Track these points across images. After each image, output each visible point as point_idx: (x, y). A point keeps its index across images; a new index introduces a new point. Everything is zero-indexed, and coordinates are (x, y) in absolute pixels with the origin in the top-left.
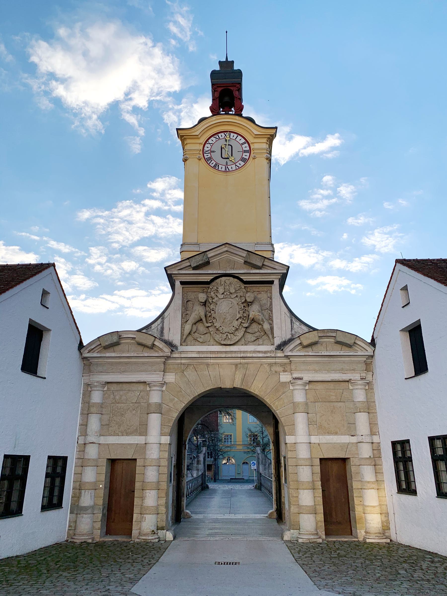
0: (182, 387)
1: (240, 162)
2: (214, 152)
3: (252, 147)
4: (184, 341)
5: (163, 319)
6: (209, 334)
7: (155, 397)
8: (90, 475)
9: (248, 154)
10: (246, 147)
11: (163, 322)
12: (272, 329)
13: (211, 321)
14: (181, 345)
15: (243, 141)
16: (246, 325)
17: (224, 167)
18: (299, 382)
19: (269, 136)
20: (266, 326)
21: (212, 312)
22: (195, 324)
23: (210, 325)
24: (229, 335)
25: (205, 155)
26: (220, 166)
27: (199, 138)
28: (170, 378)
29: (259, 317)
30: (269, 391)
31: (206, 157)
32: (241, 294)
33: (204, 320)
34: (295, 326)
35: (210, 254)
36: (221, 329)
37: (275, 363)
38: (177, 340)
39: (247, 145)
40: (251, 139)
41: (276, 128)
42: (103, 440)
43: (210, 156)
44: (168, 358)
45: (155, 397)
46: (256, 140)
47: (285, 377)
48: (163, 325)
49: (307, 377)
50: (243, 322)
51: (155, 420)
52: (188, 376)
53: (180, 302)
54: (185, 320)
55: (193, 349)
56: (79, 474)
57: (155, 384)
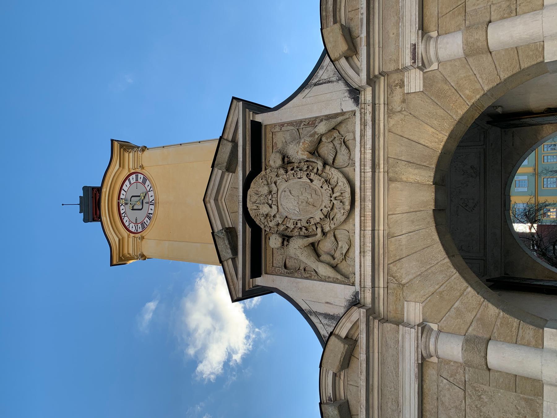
0: (432, 290)
1: (146, 185)
3: (132, 171)
4: (346, 279)
5: (311, 312)
6: (337, 232)
9: (139, 175)
10: (133, 178)
11: (316, 314)
12: (328, 117)
13: (314, 228)
14: (353, 284)
16: (320, 165)
18: (421, 49)
19: (122, 150)
20: (322, 128)
21: (299, 225)
22: (318, 256)
23: (319, 230)
24: (334, 195)
25: (139, 231)
26: (150, 212)
27: (123, 238)
28: (414, 312)
29: (307, 141)
30: (440, 112)
32: (273, 175)
33: (311, 240)
34: (325, 77)
35: (218, 226)
36: (325, 211)
37: (387, 104)
39: (131, 177)
40: (125, 173)
41: (112, 141)
43: (140, 225)
44: (372, 313)
45: (452, 349)
46: (127, 167)
47: (414, 82)
48: (321, 314)
49: (411, 34)
50: (315, 170)
52: (411, 277)
53: (286, 279)
54: (314, 273)
55: (361, 264)
57: (422, 346)
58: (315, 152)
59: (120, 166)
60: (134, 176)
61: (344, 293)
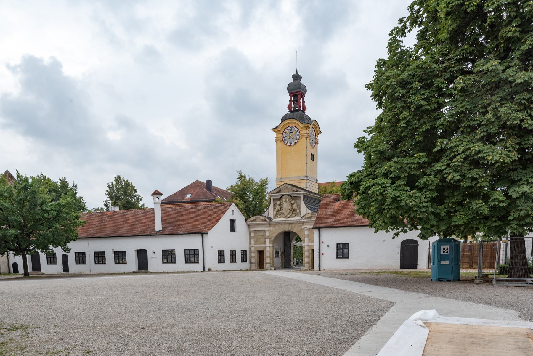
7: (267, 234)
8: (253, 255)
20: (298, 211)
28: (271, 228)
29: (296, 208)
38: (272, 217)
42: (255, 246)
51: (268, 241)
56: (250, 254)
58: (294, 210)
61: (272, 217)
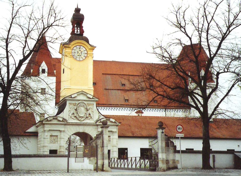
2: (75, 53)
9: (86, 55)
15: (85, 49)
17: (78, 59)
31: (73, 55)
39: (86, 51)
40: (88, 50)
59: (90, 49)
60: (86, 52)
